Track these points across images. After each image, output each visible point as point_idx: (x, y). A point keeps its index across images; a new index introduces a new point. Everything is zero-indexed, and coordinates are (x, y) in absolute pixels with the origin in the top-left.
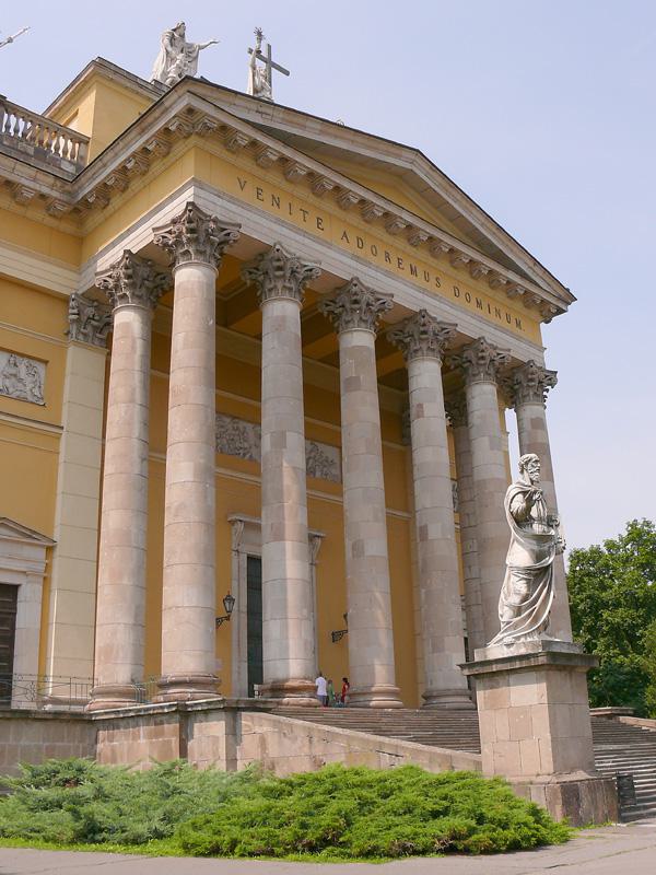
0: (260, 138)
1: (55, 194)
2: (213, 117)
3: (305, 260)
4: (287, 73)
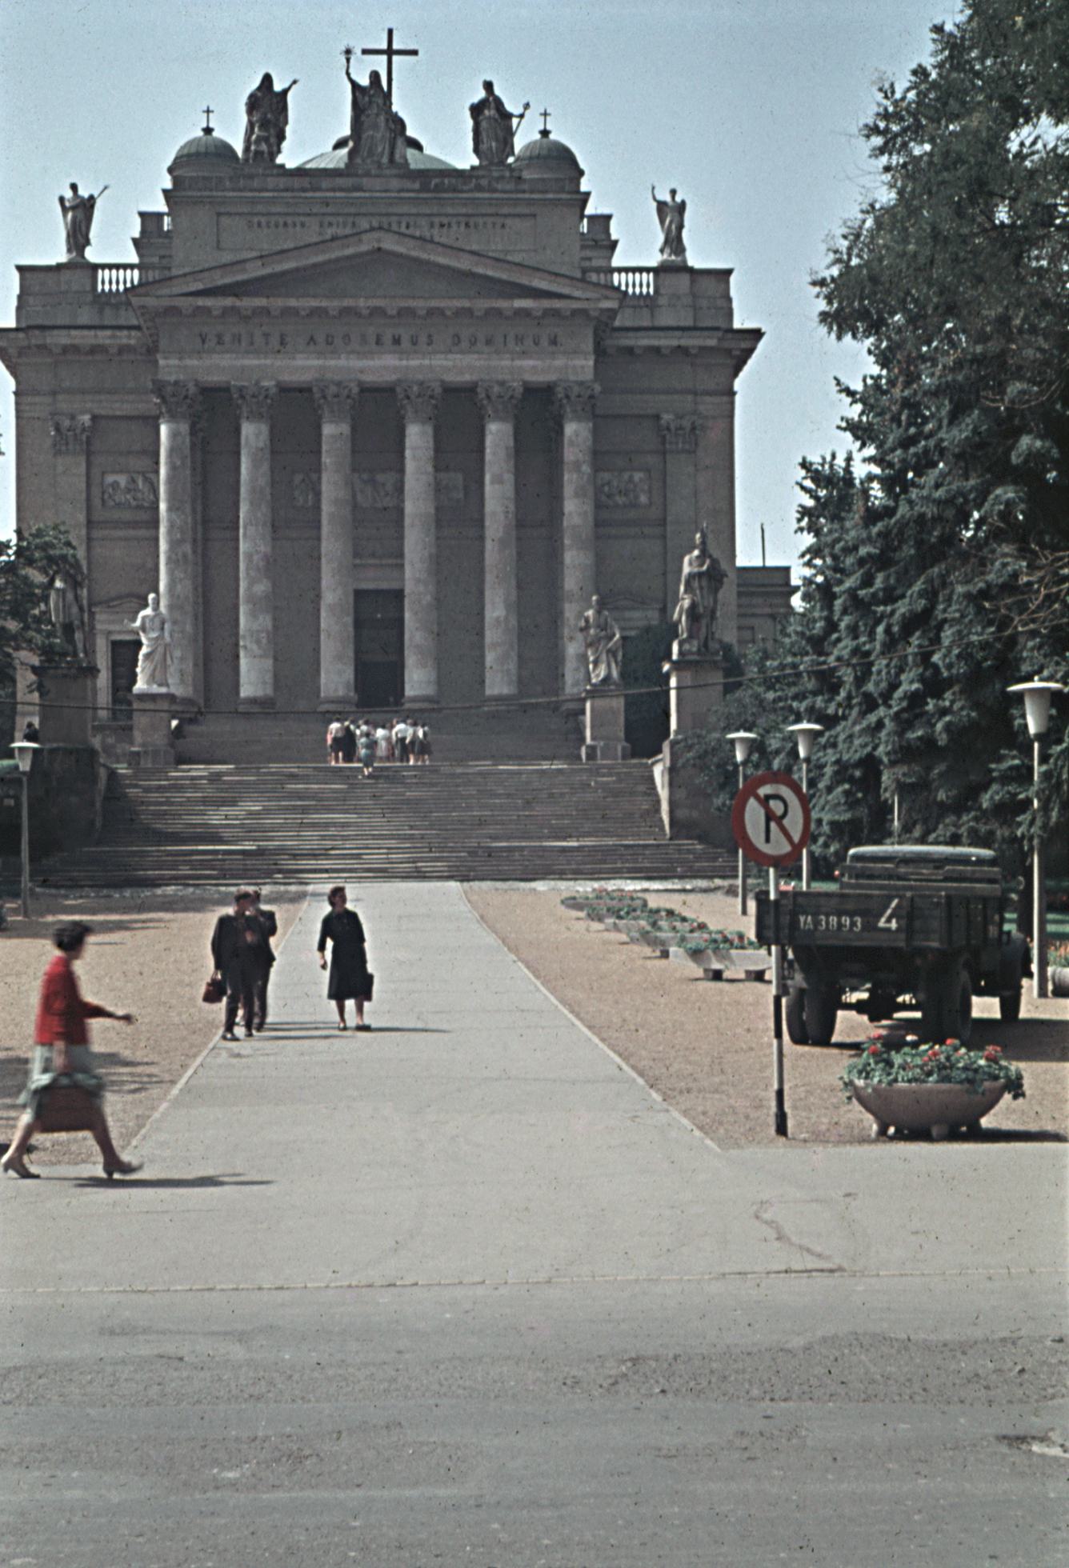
0: (201, 302)
4: (414, 53)
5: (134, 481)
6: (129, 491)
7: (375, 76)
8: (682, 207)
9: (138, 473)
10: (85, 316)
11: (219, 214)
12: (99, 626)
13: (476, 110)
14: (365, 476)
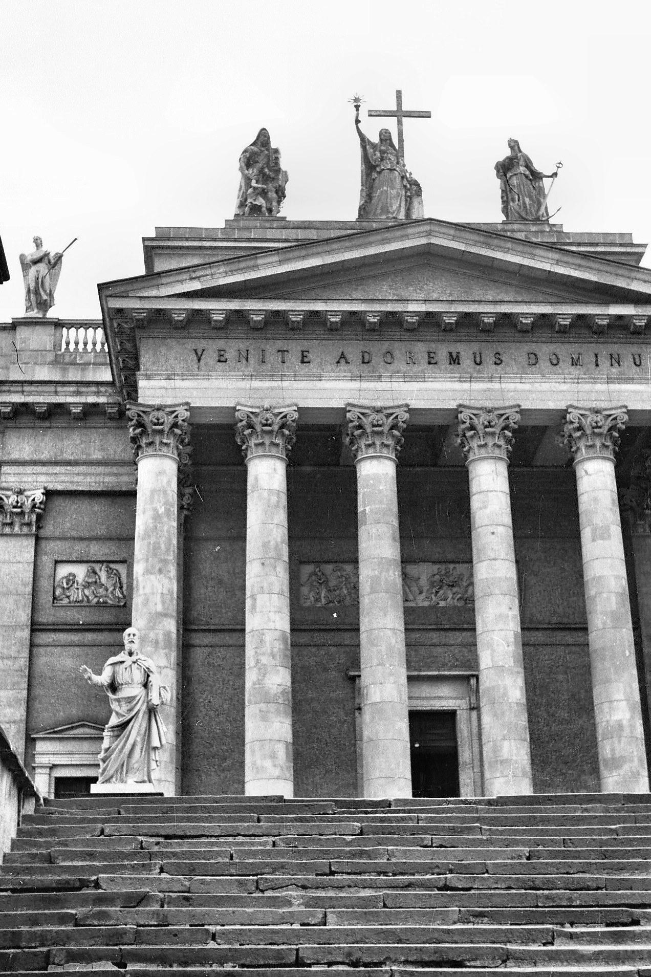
1: (102, 400)
2: (139, 309)
5: (94, 572)
6: (87, 585)
7: (385, 137)
9: (101, 562)
12: (40, 760)
13: (505, 169)
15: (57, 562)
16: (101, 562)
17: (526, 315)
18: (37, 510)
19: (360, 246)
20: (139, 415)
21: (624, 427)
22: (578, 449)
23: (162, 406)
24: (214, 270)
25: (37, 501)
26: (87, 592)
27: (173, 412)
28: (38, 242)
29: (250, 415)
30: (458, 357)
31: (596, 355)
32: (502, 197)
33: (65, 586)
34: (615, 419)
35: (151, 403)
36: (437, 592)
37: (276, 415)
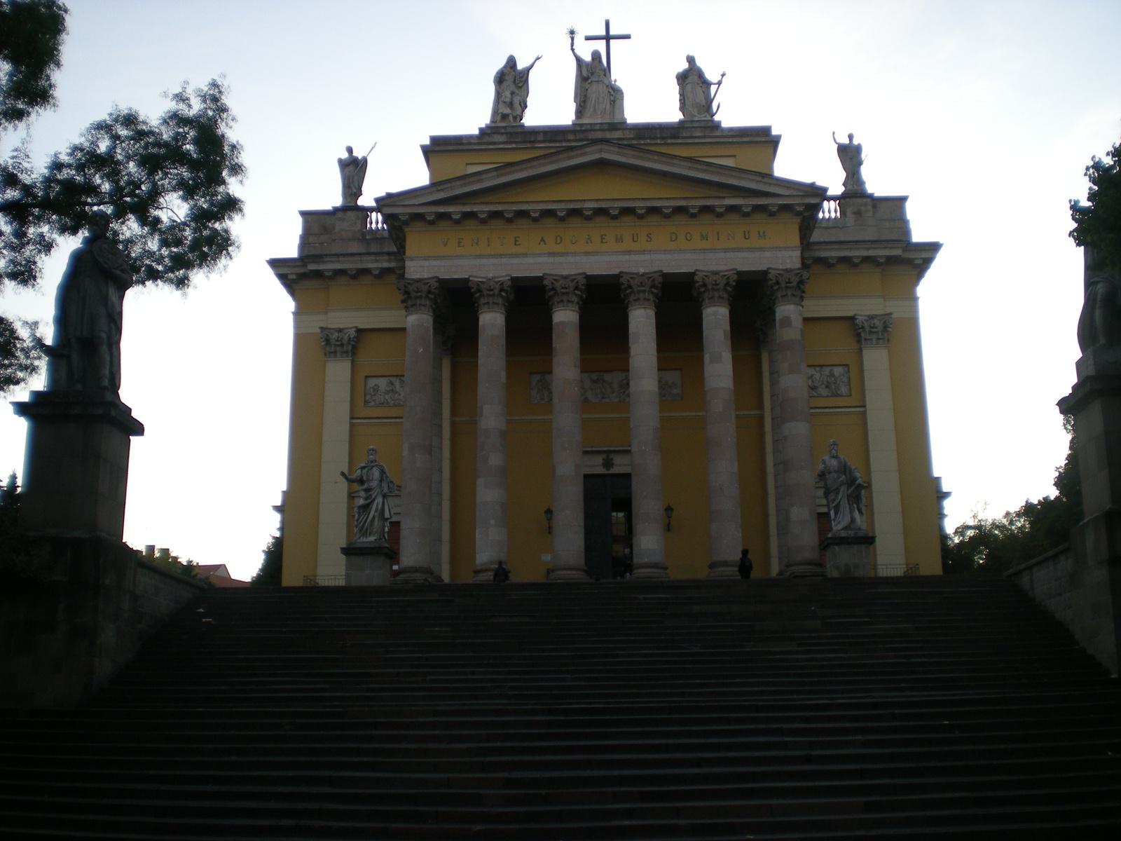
0: (442, 209)
1: (393, 265)
3: (495, 278)
4: (627, 37)
5: (391, 383)
6: (387, 392)
7: (596, 55)
8: (858, 149)
9: (397, 376)
10: (355, 247)
11: (467, 164)
13: (682, 78)
14: (594, 376)
15: (366, 377)
16: (397, 376)
17: (667, 207)
18: (352, 343)
19: (551, 163)
20: (405, 286)
21: (734, 284)
22: (703, 300)
23: (420, 279)
24: (454, 184)
25: (352, 336)
26: (387, 397)
27: (428, 283)
28: (350, 150)
29: (480, 283)
30: (621, 238)
31: (718, 233)
32: (680, 100)
33: (373, 394)
34: (728, 278)
35: (414, 277)
36: (624, 392)
37: (497, 283)
